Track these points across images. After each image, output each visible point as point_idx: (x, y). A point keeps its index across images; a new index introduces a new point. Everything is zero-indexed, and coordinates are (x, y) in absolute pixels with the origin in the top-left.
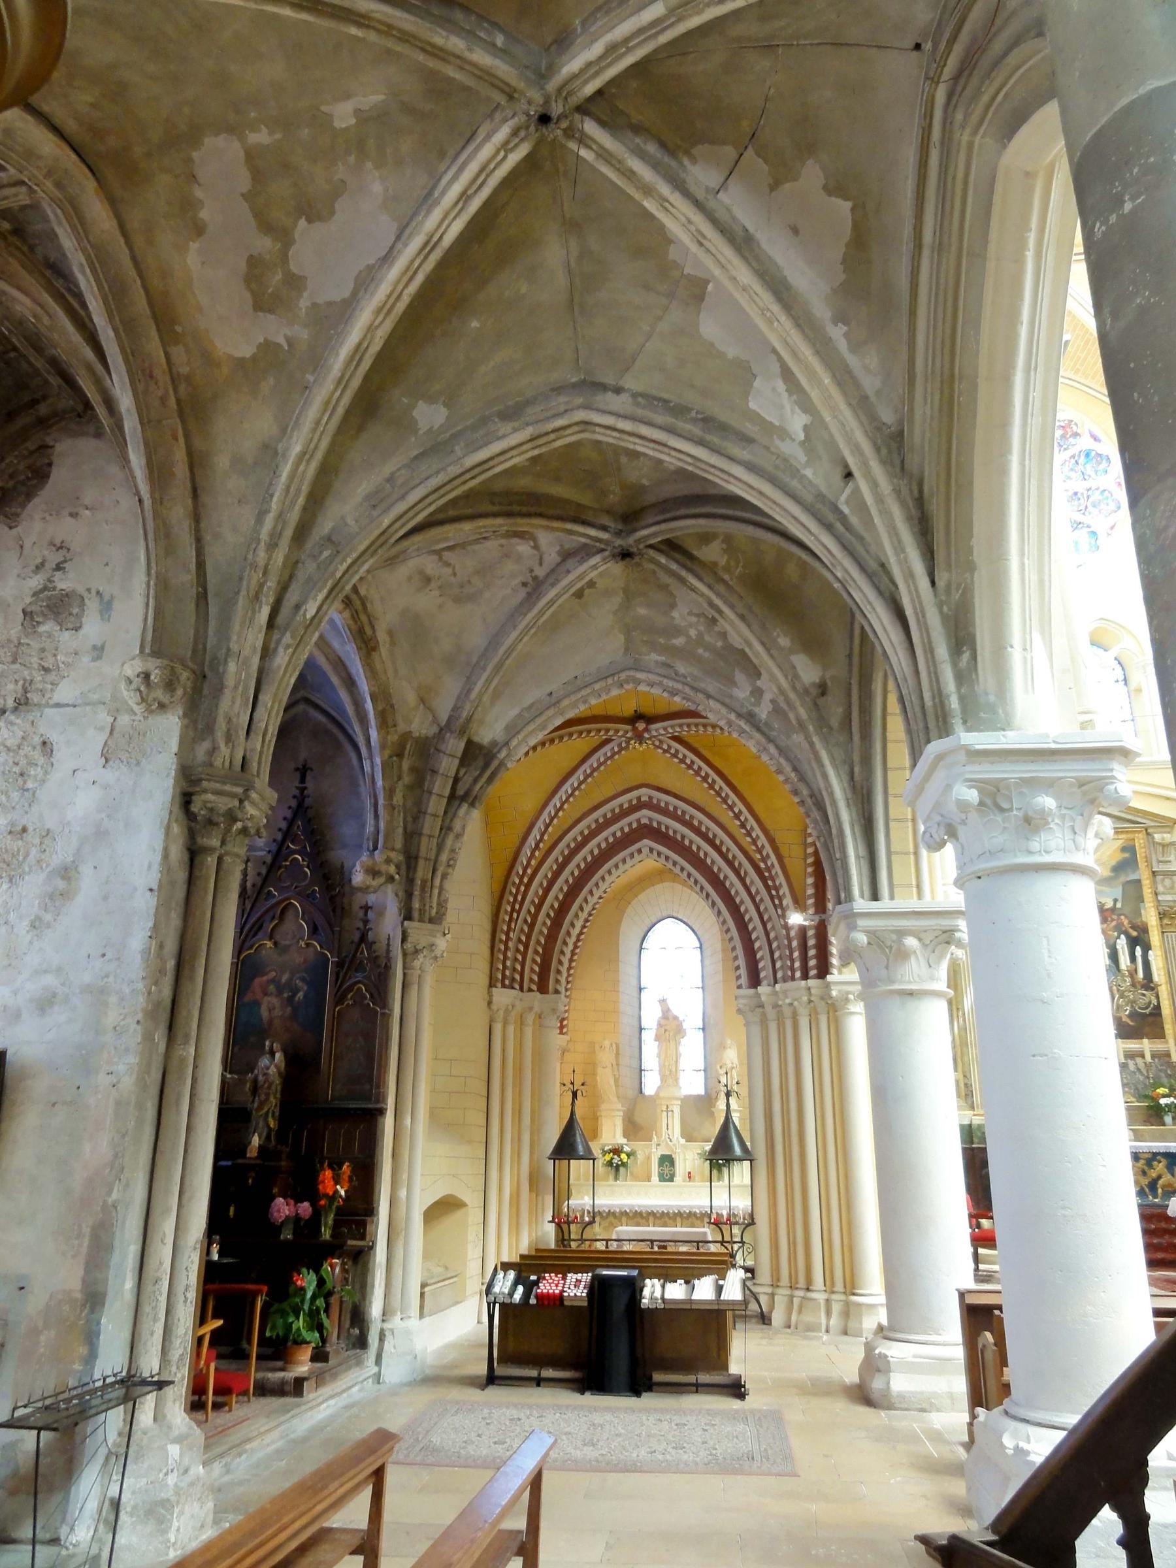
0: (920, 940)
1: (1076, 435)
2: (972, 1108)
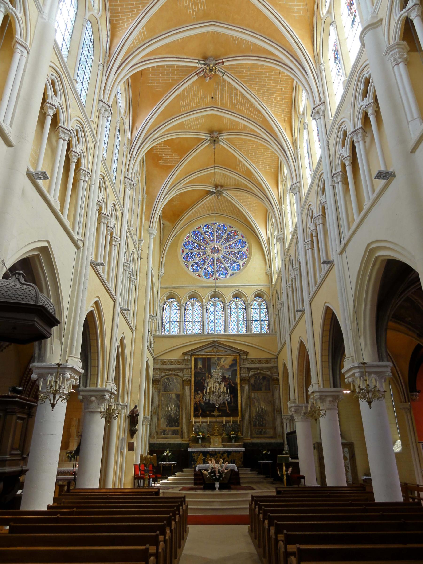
0: (96, 398)
1: (237, 235)
2: (182, 438)
